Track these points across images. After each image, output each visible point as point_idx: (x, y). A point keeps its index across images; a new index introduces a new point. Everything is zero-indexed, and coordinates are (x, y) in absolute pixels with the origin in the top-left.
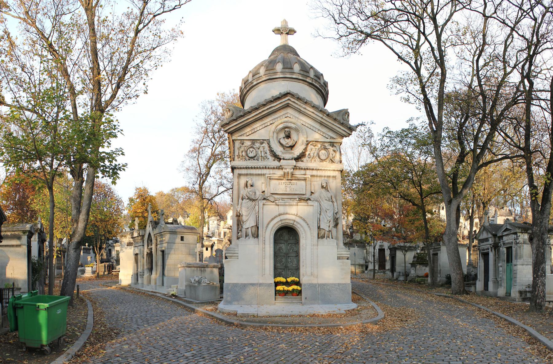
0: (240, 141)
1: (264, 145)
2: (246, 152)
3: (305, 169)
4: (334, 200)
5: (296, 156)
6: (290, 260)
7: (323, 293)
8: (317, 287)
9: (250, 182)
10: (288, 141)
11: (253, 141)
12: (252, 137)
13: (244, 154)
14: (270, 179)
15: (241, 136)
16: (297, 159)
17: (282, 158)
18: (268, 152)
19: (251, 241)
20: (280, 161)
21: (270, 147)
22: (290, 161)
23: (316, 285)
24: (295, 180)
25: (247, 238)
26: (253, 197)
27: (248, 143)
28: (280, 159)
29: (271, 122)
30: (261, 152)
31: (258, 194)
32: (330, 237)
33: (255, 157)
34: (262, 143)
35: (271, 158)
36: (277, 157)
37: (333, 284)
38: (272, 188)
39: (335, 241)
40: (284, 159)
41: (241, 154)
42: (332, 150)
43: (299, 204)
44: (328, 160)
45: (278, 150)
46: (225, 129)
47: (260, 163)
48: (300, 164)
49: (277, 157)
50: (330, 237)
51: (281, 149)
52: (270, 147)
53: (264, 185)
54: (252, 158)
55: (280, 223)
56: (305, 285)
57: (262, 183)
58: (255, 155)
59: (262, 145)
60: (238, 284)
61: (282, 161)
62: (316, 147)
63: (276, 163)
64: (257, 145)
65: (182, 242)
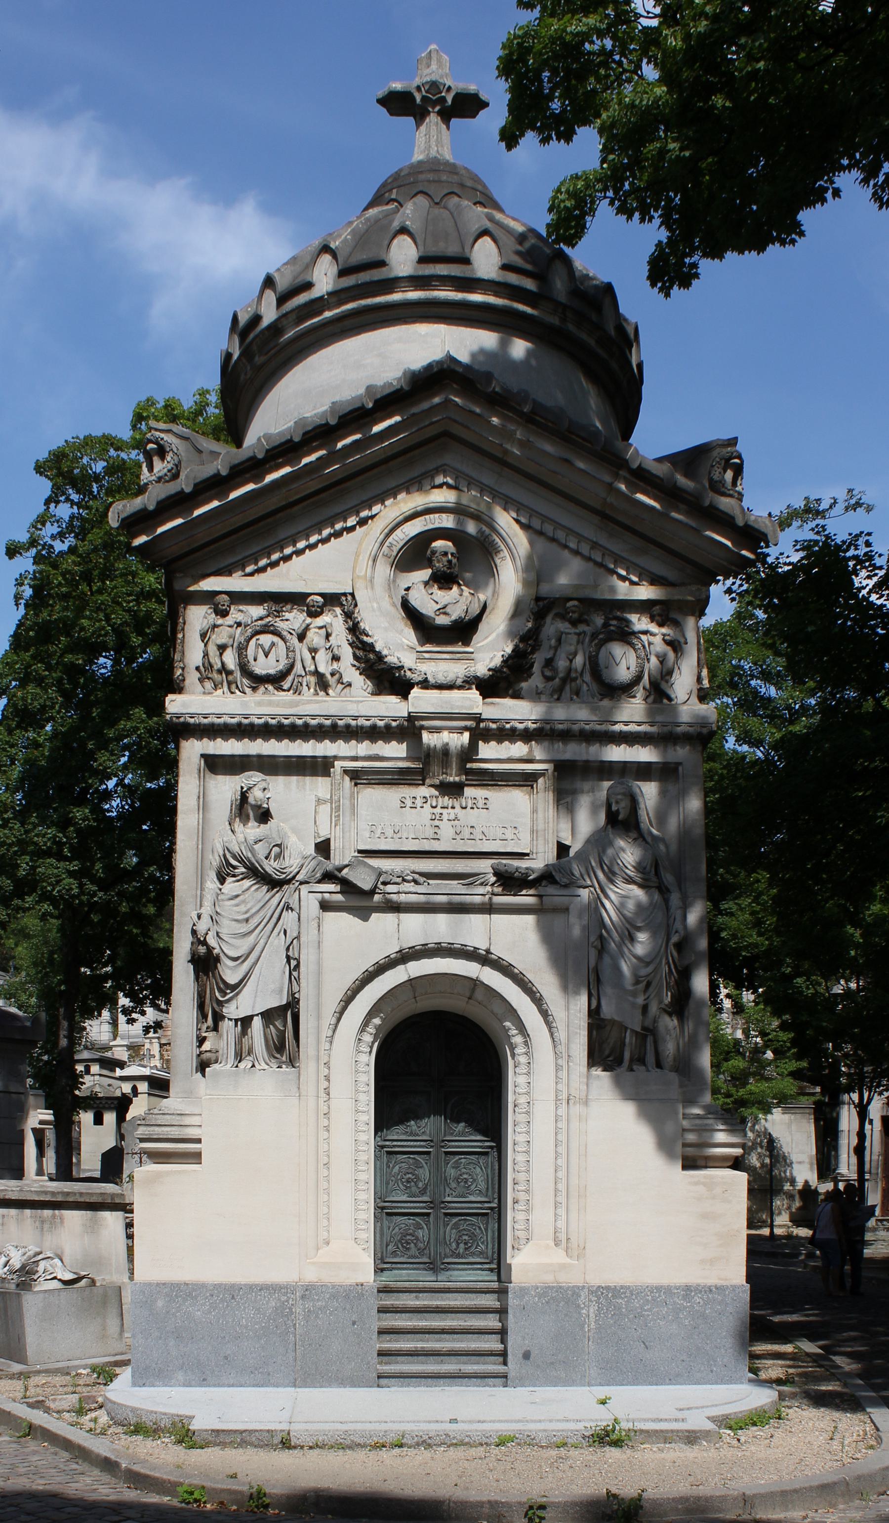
1: (325, 619)
2: (241, 650)
4: (668, 878)
6: (452, 1172)
7: (618, 1329)
9: (256, 795)
10: (443, 596)
13: (230, 659)
17: (416, 678)
18: (347, 654)
19: (264, 1080)
20: (405, 695)
22: (456, 693)
23: (575, 1291)
25: (246, 1064)
26: (270, 867)
30: (313, 651)
31: (299, 854)
32: (650, 1058)
35: (360, 683)
37: (659, 1289)
38: (364, 826)
39: (674, 1077)
40: (425, 684)
42: (658, 640)
45: (397, 643)
47: (309, 705)
50: (650, 1058)
51: (409, 636)
53: (325, 809)
56: (523, 1291)
57: (319, 801)
58: (281, 666)
60: (203, 1286)
61: (415, 692)
62: (582, 628)
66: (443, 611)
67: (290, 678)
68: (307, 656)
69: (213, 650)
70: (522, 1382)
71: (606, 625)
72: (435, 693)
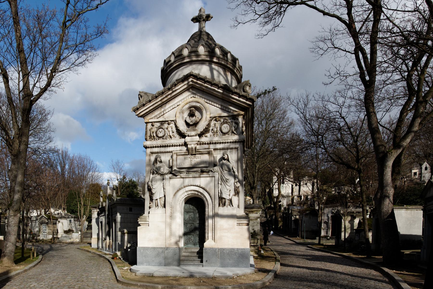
0: (151, 124)
2: (156, 132)
3: (208, 144)
5: (199, 133)
8: (217, 251)
11: (162, 123)
12: (161, 119)
14: (177, 155)
15: (152, 118)
16: (200, 135)
17: (187, 135)
19: (160, 210)
21: (176, 127)
24: (200, 154)
27: (158, 124)
28: (186, 136)
29: (178, 104)
33: (163, 136)
34: (169, 124)
35: (178, 136)
36: (182, 135)
40: (188, 136)
41: (152, 135)
43: (201, 176)
44: (230, 133)
46: (137, 114)
48: (204, 139)
49: (182, 135)
52: (176, 127)
54: (160, 137)
55: (186, 194)
56: (206, 249)
59: (170, 126)
60: (149, 248)
61: (187, 138)
63: (182, 141)
64: (166, 125)
65: (131, 212)
66: (192, 122)
67: (165, 137)
68: (168, 132)
69: (151, 132)
70: (206, 266)
71: (224, 121)
72: (190, 137)
